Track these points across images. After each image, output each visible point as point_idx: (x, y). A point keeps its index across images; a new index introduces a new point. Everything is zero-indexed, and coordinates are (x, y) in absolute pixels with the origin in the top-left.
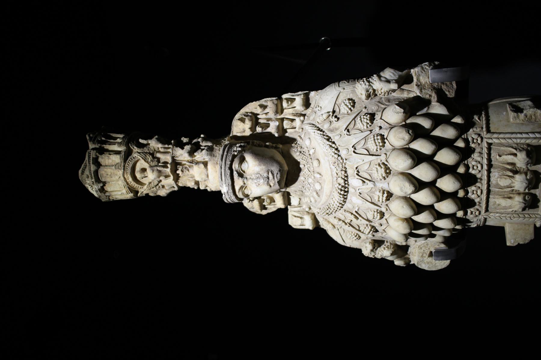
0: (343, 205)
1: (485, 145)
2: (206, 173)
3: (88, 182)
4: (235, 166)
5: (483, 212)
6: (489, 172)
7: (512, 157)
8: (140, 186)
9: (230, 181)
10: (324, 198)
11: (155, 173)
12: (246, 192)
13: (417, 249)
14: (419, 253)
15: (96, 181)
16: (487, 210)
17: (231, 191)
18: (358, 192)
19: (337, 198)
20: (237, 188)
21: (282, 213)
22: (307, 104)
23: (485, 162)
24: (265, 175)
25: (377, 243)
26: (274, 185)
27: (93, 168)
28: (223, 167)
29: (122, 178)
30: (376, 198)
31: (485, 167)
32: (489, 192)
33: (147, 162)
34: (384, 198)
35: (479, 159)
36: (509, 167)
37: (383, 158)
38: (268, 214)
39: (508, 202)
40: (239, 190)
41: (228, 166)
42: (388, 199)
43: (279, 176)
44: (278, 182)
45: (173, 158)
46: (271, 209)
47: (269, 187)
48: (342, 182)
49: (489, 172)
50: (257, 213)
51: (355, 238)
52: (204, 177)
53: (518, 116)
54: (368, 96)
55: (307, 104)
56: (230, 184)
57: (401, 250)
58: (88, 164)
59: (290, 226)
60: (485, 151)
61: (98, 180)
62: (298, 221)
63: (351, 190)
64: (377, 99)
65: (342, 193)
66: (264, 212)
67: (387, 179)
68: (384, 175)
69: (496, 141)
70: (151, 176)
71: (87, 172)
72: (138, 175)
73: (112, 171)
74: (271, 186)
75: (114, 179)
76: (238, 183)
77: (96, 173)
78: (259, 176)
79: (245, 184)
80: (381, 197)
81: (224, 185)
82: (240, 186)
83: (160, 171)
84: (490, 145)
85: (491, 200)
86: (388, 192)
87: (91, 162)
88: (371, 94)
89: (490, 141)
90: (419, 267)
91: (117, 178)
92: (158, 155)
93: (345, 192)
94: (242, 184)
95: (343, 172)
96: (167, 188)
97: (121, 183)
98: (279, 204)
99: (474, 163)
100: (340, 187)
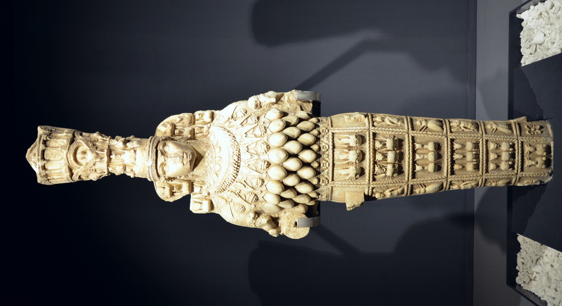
1: (330, 134)
2: (132, 159)
3: (33, 160)
4: (160, 147)
5: (330, 180)
6: (333, 151)
7: (347, 139)
8: (78, 166)
10: (221, 176)
11: (94, 155)
13: (286, 219)
14: (287, 222)
15: (41, 159)
16: (333, 180)
17: (154, 165)
18: (247, 164)
19: (232, 171)
21: (186, 199)
22: (212, 117)
23: (331, 144)
24: (181, 155)
25: (258, 214)
26: (187, 163)
27: (42, 147)
28: (151, 147)
29: (65, 157)
30: (259, 167)
31: (331, 147)
32: (334, 164)
33: (89, 146)
34: (265, 166)
35: (327, 142)
36: (346, 146)
37: (265, 139)
38: (175, 202)
39: (346, 172)
41: (155, 146)
42: (267, 167)
43: (191, 156)
45: (109, 146)
46: (178, 196)
48: (236, 158)
49: (333, 151)
50: (166, 200)
52: (133, 160)
53: (350, 118)
54: (257, 106)
55: (212, 117)
56: (155, 159)
57: (274, 221)
58: (38, 144)
59: (191, 211)
60: (331, 137)
61: (43, 158)
62: (198, 207)
63: (242, 164)
64: (262, 109)
65: (236, 166)
66: (171, 200)
67: (268, 153)
68: (266, 149)
69: (337, 131)
70: (90, 156)
71: (35, 151)
72: (79, 156)
73: (57, 152)
75: (57, 159)
76: (161, 159)
77: (43, 151)
78: (176, 155)
80: (263, 165)
81: (150, 159)
83: (97, 154)
84: (333, 134)
85: (335, 171)
86: (268, 162)
87: (41, 142)
88: (258, 106)
89: (333, 132)
90: (287, 236)
91: (60, 158)
92: (98, 144)
93: (238, 166)
94: (163, 160)
95: (238, 152)
96: (98, 172)
97: (64, 161)
98: (185, 191)
99: (323, 144)
100: (235, 162)
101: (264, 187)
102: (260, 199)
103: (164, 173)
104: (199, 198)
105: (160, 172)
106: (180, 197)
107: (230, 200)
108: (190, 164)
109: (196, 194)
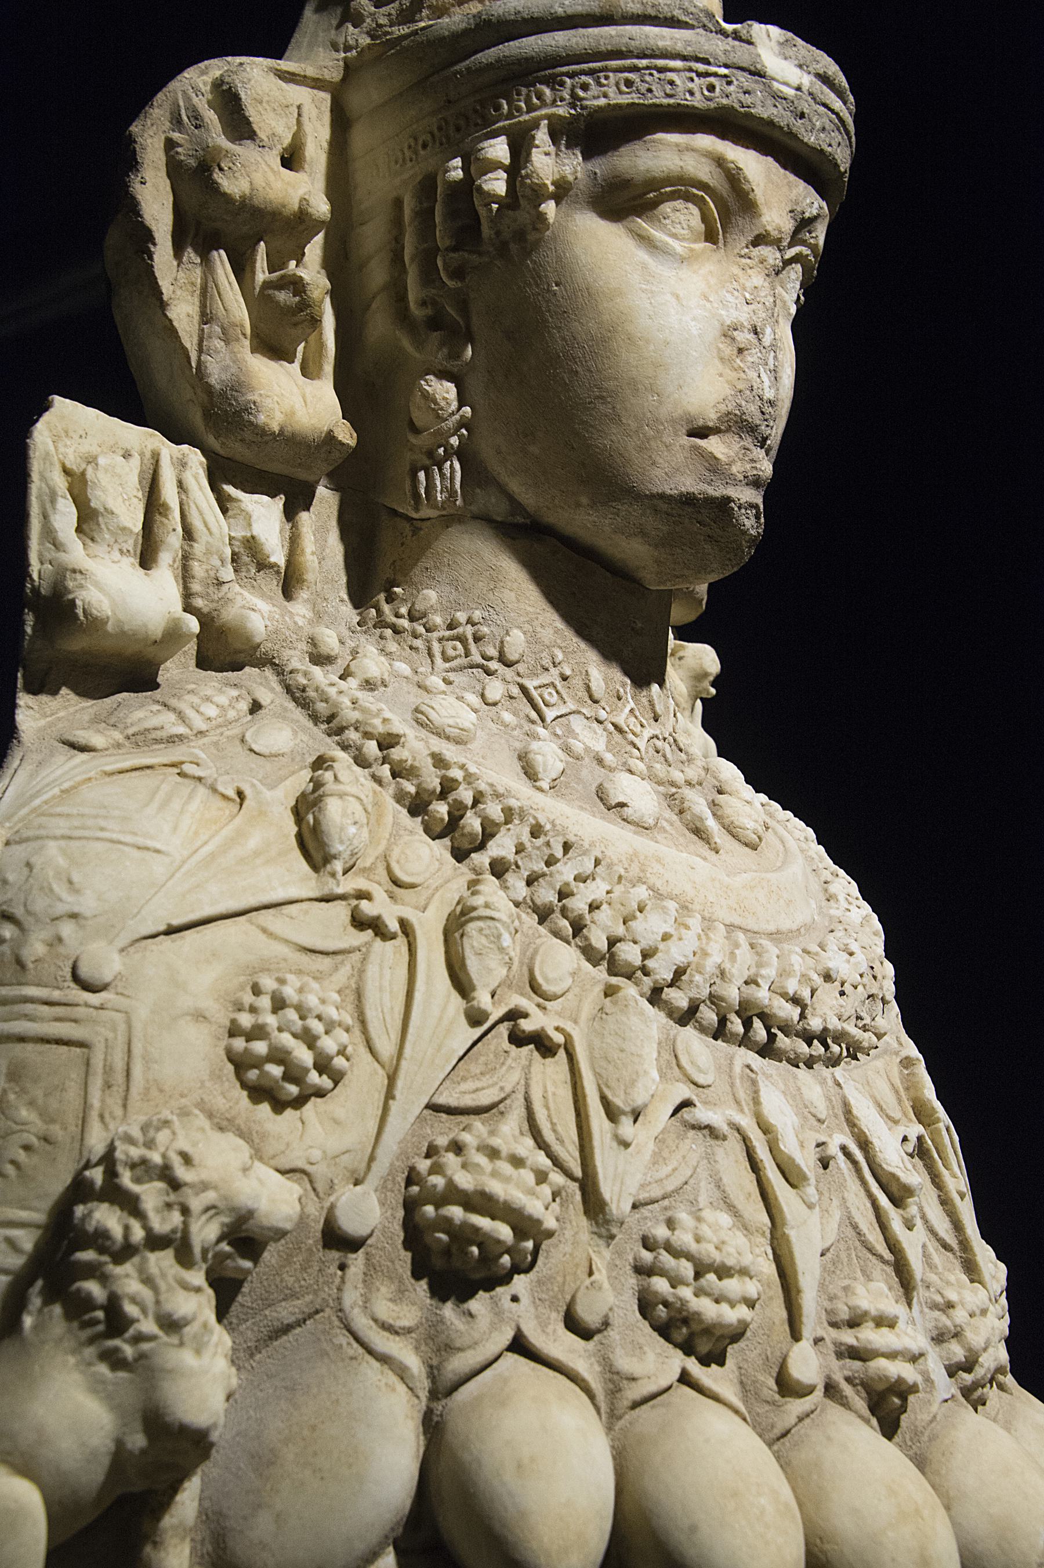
0: (655, 996)
9: (811, 139)
12: (682, 219)
20: (755, 167)
26: (714, 467)
40: (734, 177)
44: (728, 500)
46: (192, 297)
47: (712, 418)
50: (151, 136)
51: (304, 1056)
56: (799, 126)
74: (701, 432)
79: (758, 241)
82: (759, 194)
101: (658, 1363)
102: (484, 1322)
103: (625, 201)
104: (188, 534)
105: (670, 153)
106: (183, 312)
107: (381, 906)
108: (688, 500)
109: (224, 503)
